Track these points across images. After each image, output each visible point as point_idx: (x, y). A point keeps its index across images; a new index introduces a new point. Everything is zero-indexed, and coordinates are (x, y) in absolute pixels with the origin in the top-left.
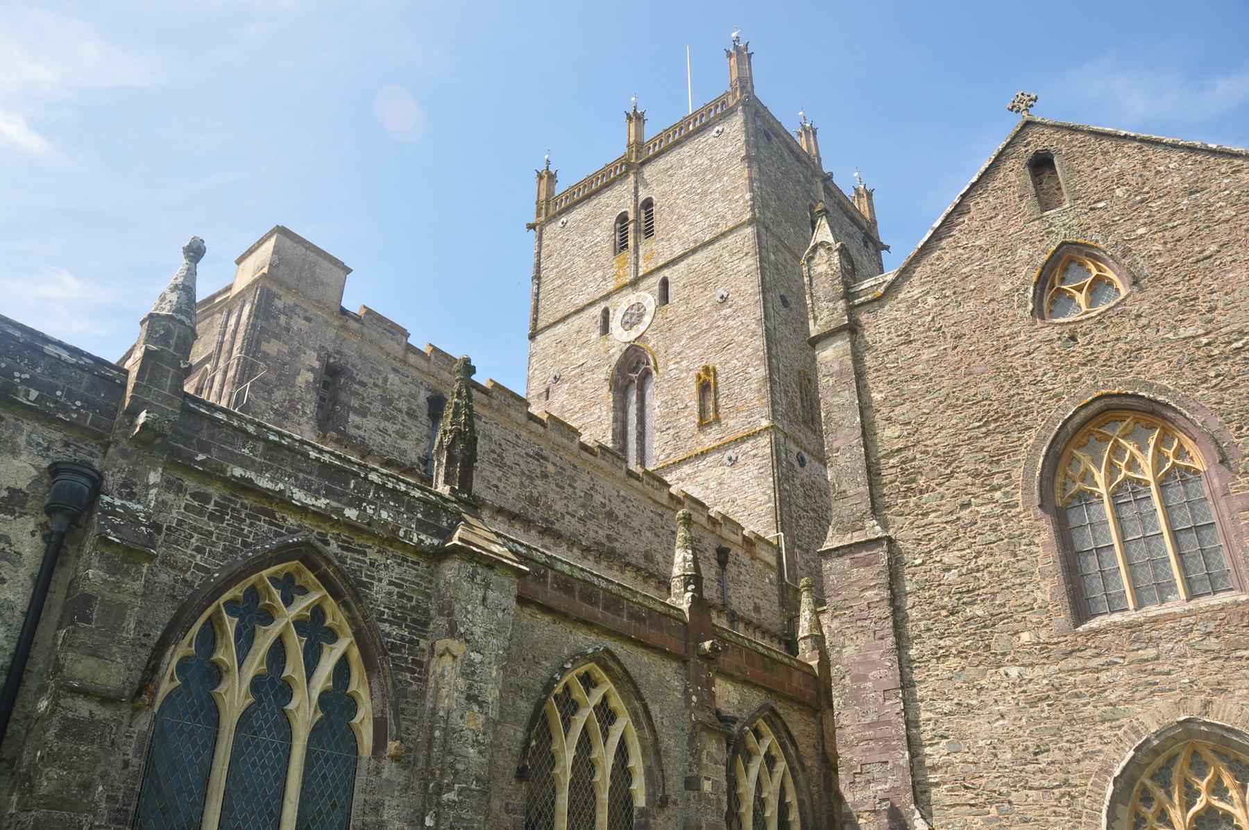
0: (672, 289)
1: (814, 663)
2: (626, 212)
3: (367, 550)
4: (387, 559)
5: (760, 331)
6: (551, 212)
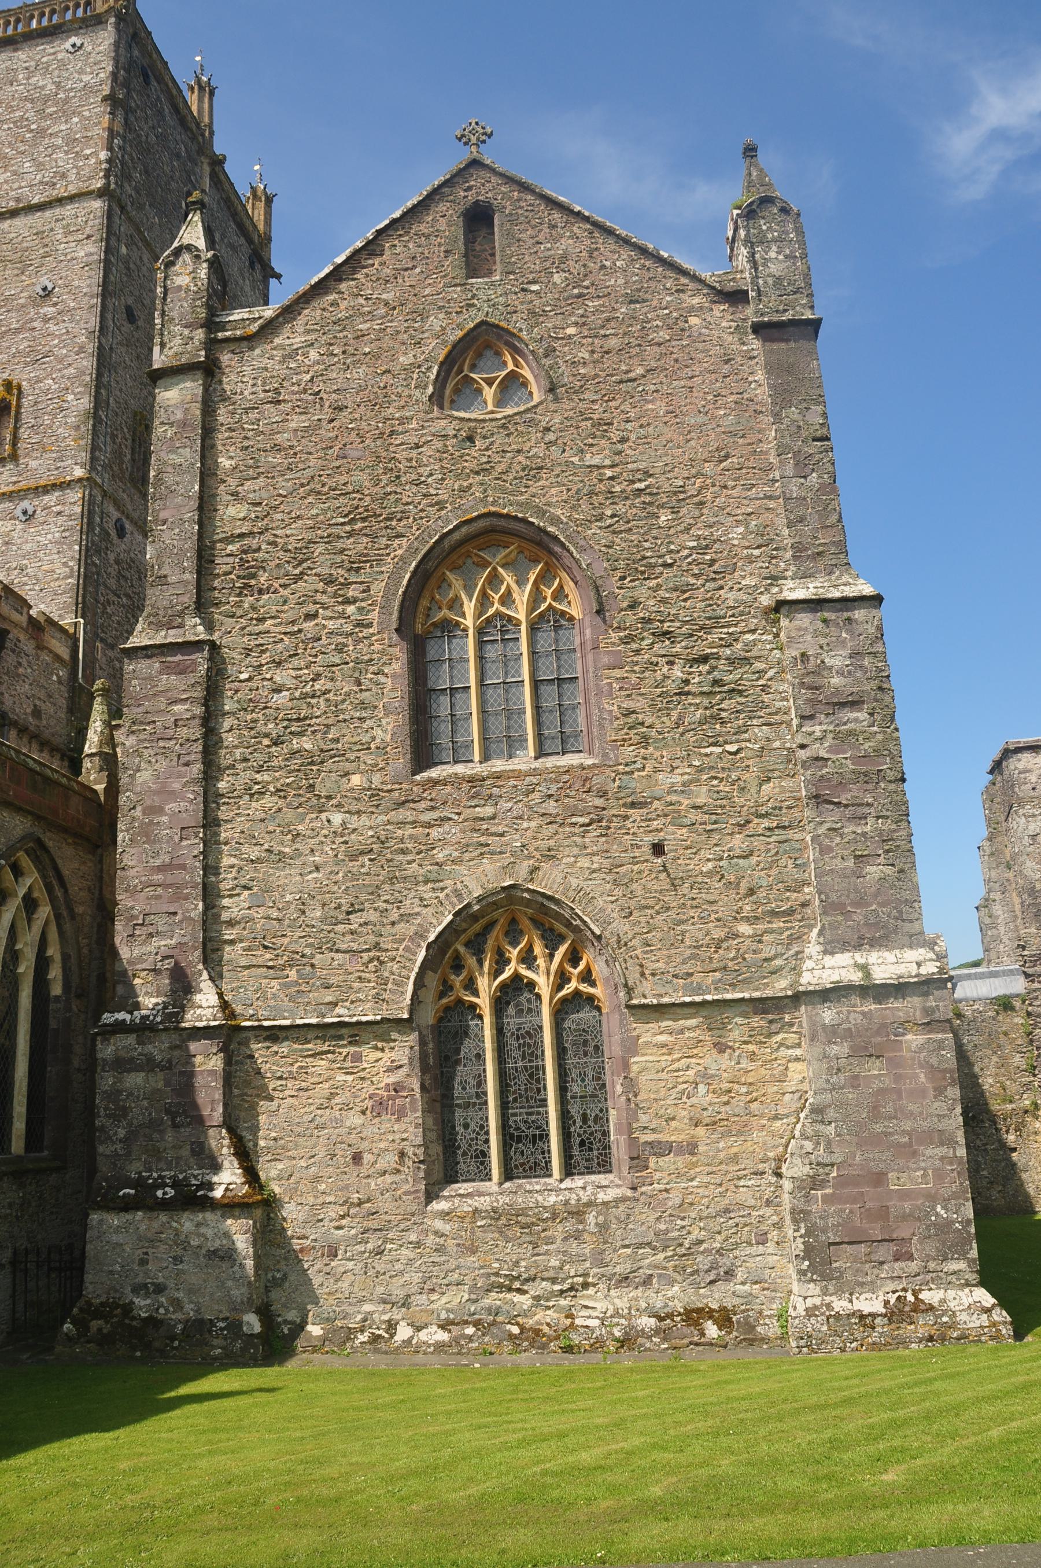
1: (100, 787)
5: (91, 347)
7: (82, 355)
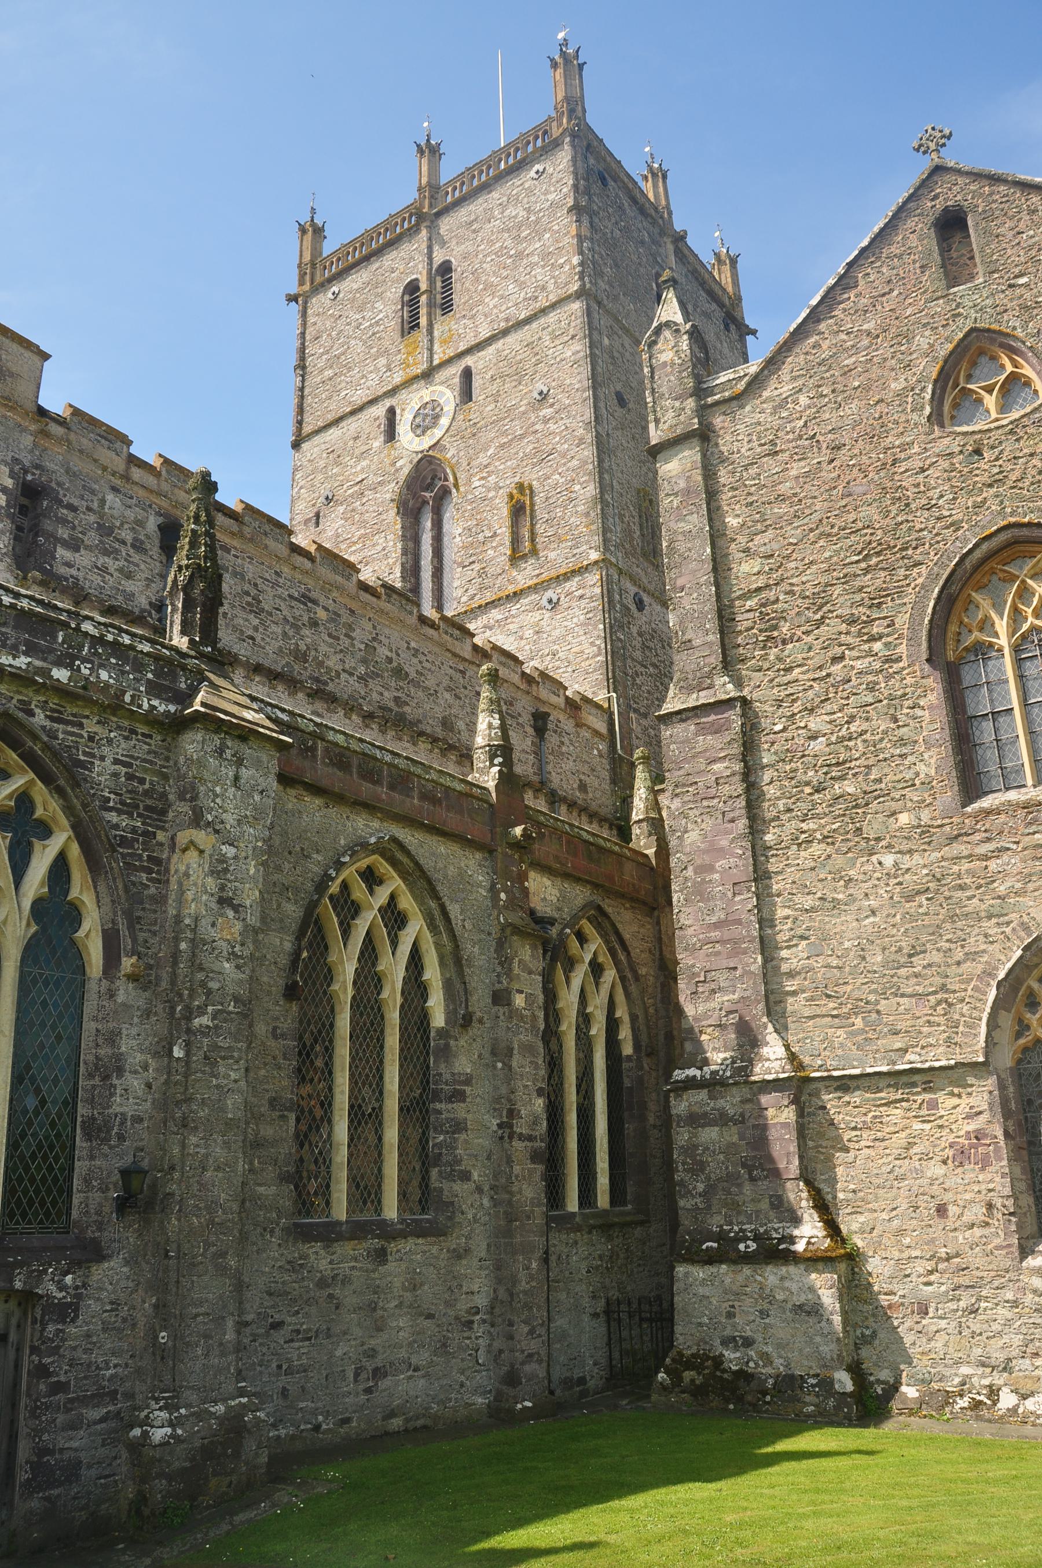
0: (477, 382)
1: (651, 852)
2: (417, 279)
3: (84, 721)
4: (110, 731)
5: (589, 438)
6: (318, 279)
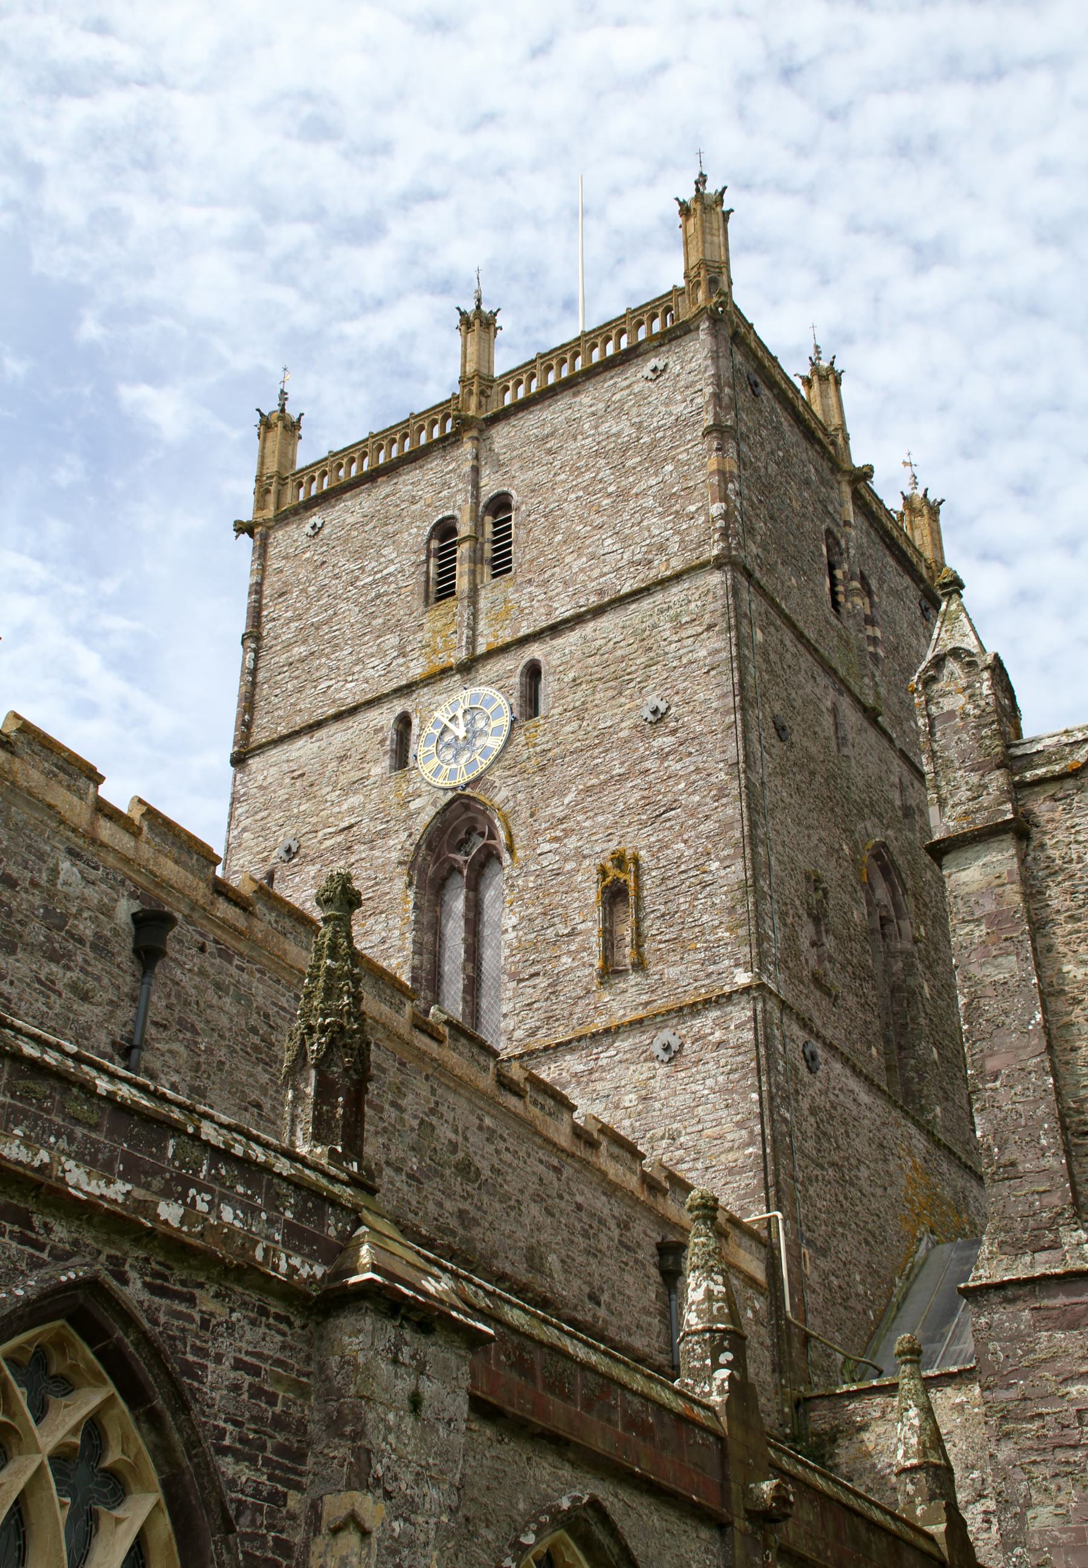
0: (547, 687)
1: (938, 1529)
2: (452, 518)
3: (197, 1292)
4: (232, 1310)
5: (734, 788)
6: (288, 502)
7: (724, 800)
